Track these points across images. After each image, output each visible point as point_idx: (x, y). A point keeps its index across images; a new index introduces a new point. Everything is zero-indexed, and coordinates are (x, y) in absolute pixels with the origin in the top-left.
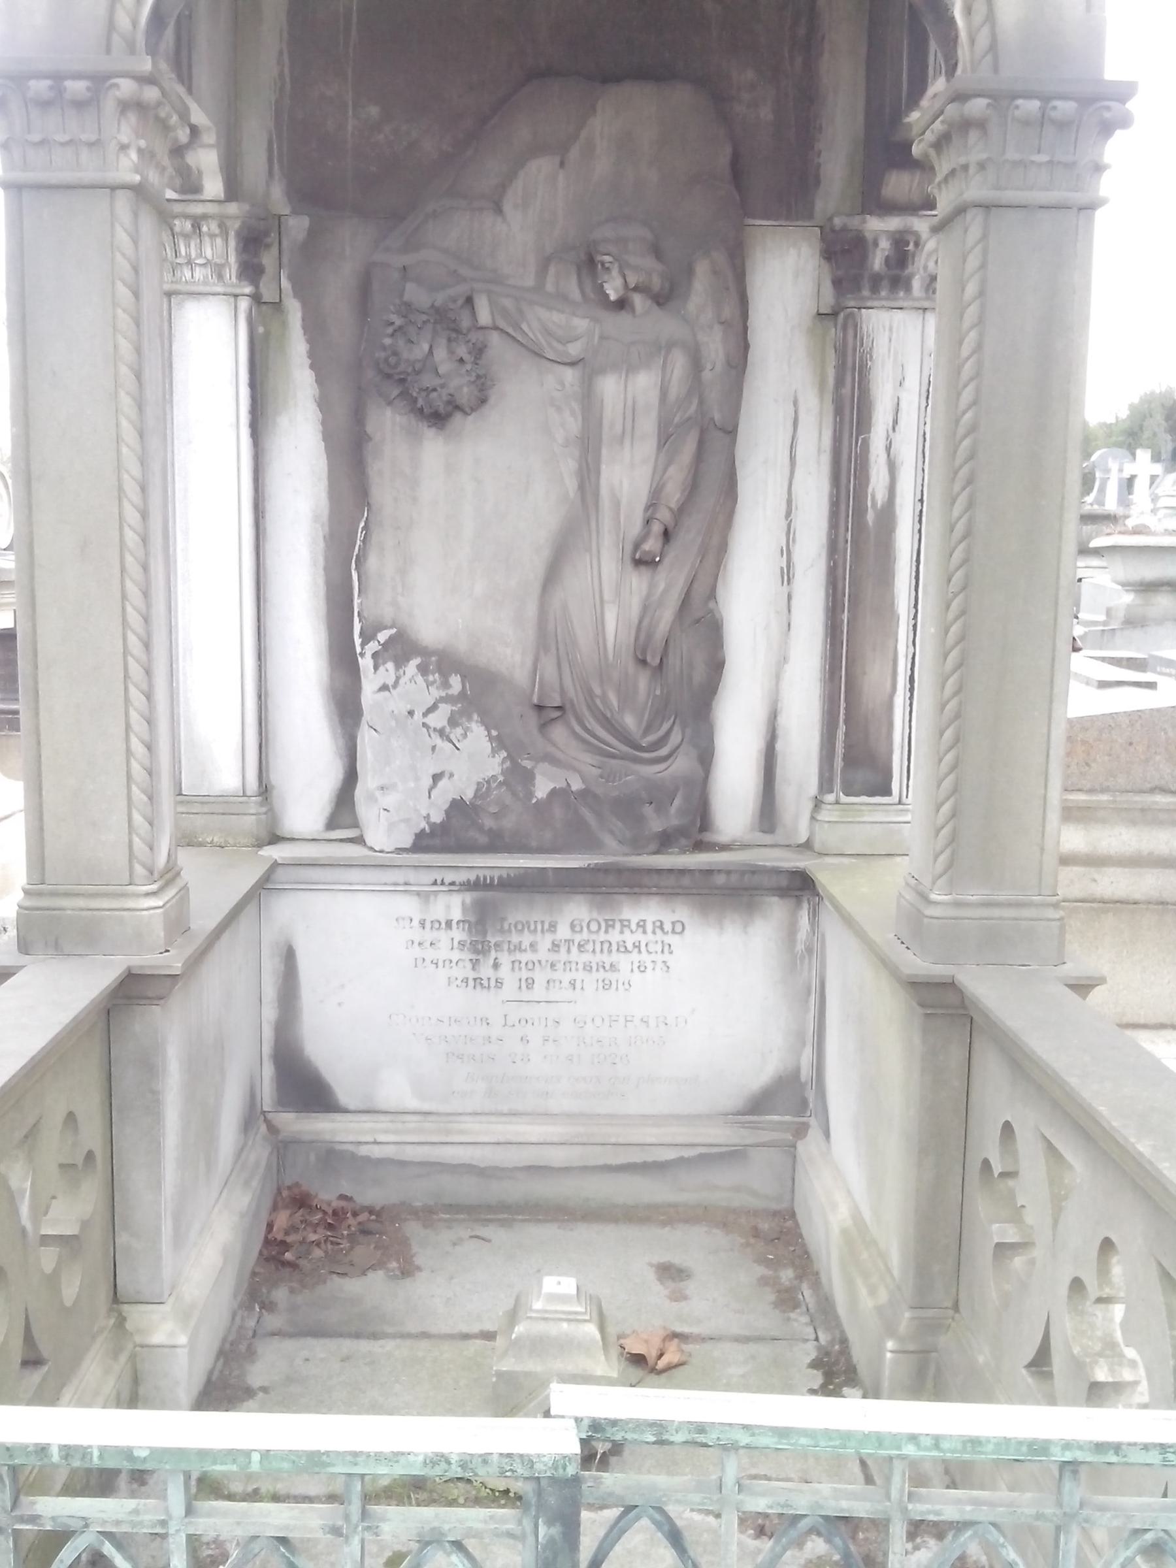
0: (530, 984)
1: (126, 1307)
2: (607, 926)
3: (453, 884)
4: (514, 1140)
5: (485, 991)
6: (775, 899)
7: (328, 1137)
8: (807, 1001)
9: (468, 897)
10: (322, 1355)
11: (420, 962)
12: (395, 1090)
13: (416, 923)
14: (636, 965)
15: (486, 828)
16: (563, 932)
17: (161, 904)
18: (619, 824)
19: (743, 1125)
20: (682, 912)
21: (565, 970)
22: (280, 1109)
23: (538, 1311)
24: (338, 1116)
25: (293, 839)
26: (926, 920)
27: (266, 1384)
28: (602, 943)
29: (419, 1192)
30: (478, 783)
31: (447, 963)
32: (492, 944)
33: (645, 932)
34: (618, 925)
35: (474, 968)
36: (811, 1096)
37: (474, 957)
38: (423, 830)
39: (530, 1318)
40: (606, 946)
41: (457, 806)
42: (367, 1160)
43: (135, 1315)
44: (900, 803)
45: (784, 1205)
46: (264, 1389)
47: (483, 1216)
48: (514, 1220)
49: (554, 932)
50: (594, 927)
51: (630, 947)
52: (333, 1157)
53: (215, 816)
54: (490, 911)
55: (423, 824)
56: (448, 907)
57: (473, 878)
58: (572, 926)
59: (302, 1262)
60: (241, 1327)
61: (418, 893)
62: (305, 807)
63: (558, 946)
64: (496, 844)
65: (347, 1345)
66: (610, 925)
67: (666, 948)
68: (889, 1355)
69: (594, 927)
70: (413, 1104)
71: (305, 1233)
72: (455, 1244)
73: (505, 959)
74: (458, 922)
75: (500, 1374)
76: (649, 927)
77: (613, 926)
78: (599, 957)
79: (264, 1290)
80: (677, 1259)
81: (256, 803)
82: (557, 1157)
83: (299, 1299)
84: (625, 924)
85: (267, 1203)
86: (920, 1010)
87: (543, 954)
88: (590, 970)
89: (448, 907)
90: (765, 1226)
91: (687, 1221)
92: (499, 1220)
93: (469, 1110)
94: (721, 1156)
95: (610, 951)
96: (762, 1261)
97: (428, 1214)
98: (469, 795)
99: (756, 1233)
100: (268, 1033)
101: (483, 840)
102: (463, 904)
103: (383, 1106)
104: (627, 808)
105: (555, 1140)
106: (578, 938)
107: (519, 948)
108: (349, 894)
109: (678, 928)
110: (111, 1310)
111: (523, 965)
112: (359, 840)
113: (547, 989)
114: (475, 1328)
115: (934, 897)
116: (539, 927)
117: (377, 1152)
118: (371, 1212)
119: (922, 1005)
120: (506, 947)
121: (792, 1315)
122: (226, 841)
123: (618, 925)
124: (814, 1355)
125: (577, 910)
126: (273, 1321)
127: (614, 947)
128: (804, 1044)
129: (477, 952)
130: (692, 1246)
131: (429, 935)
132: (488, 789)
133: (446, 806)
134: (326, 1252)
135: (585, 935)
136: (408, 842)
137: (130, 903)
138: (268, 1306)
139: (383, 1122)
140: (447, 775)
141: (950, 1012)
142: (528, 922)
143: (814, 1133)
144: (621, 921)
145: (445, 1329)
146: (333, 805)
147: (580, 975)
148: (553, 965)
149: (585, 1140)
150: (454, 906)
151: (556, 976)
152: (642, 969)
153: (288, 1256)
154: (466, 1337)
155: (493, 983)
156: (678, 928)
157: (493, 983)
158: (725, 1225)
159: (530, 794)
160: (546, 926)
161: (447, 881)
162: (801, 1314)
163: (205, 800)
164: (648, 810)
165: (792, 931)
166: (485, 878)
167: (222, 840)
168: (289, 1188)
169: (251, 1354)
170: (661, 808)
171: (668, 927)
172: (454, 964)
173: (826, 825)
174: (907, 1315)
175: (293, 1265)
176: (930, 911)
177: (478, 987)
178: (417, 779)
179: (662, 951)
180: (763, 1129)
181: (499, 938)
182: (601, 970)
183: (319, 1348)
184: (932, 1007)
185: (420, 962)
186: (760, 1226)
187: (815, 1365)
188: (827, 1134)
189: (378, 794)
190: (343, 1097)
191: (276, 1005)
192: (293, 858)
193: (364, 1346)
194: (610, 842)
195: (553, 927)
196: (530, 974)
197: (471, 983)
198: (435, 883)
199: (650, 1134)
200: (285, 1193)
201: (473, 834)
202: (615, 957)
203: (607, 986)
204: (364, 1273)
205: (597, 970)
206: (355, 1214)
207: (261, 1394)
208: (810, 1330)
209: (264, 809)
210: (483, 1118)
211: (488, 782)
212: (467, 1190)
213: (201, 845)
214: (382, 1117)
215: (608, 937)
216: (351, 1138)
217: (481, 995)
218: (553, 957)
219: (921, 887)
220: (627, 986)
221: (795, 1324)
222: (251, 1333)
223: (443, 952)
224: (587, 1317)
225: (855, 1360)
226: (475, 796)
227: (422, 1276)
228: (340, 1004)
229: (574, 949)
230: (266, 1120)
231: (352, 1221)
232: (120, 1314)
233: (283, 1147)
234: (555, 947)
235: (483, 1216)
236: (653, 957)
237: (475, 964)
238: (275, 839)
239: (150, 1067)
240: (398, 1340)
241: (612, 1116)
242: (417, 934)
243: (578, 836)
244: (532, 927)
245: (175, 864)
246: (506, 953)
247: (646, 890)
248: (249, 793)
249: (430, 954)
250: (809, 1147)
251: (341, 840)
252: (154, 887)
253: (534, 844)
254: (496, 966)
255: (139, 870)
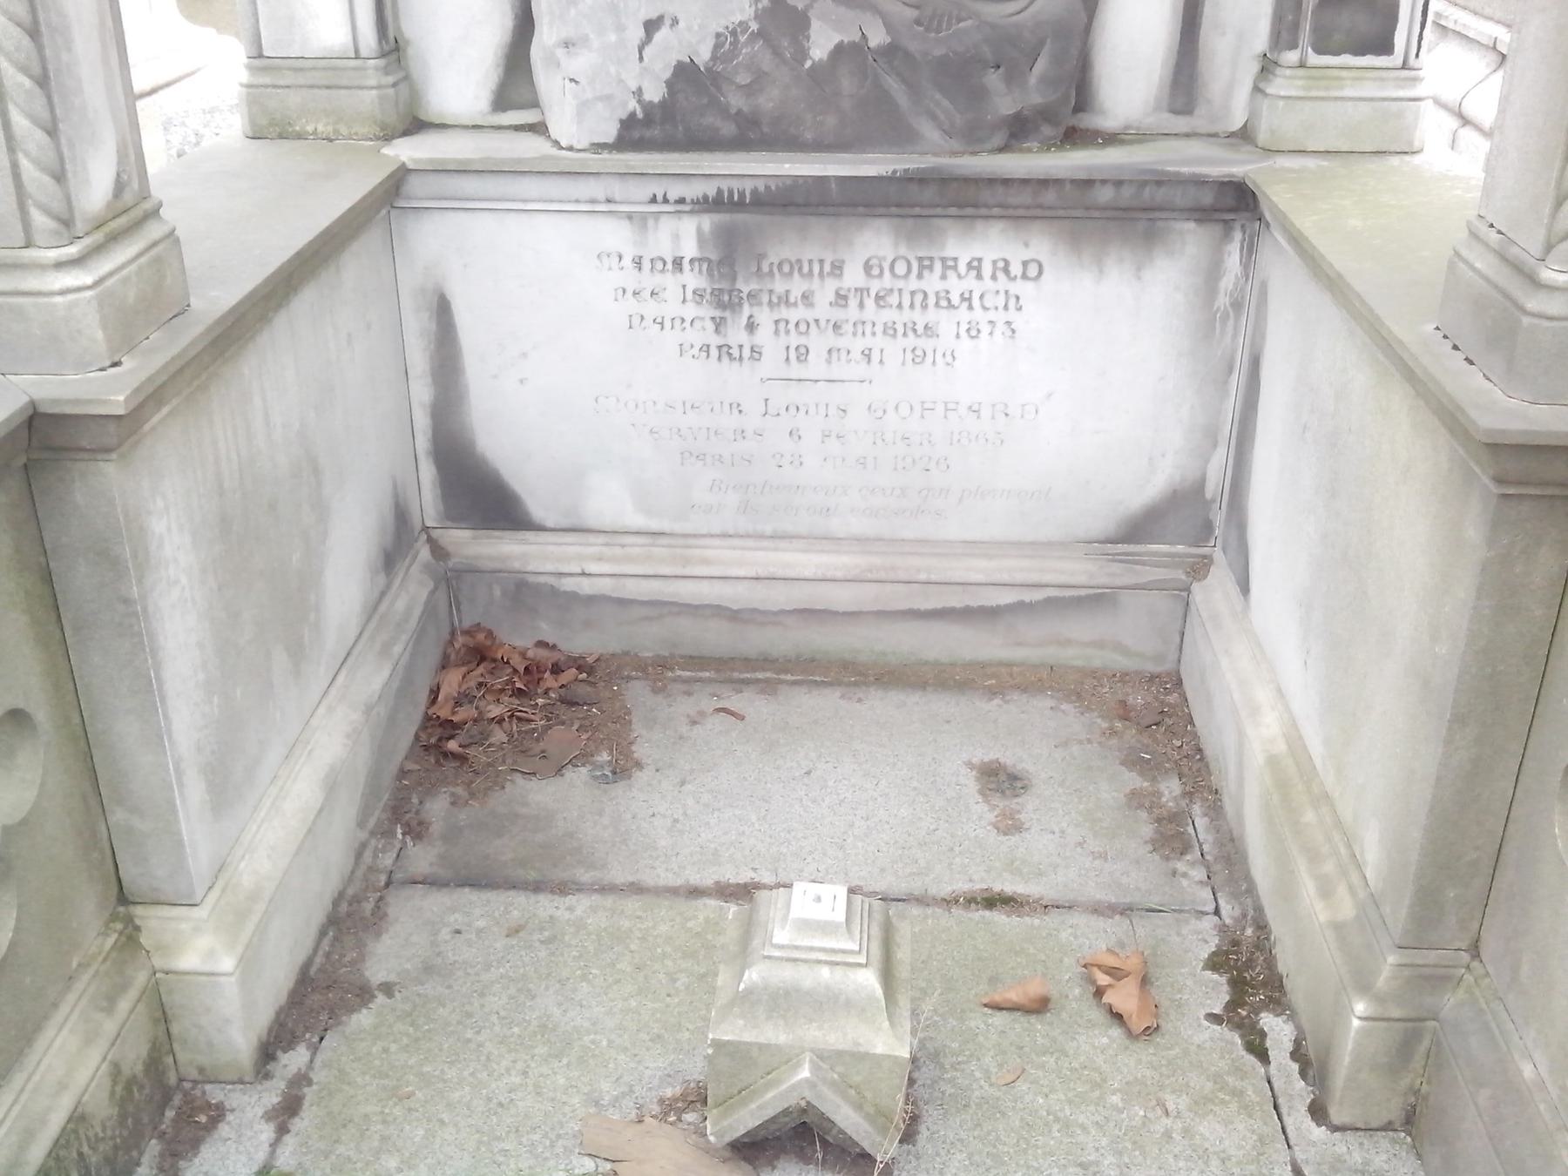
0: (803, 354)
1: (139, 911)
2: (921, 268)
3: (681, 201)
4: (780, 573)
5: (736, 364)
6: (1191, 225)
7: (517, 565)
8: (1226, 382)
9: (707, 222)
10: (481, 923)
11: (636, 321)
12: (610, 501)
13: (627, 261)
14: (964, 327)
15: (733, 111)
16: (853, 276)
17: (88, 279)
18: (946, 103)
19: (1115, 558)
20: (1039, 245)
21: (854, 334)
22: (449, 524)
23: (782, 947)
24: (530, 535)
25: (443, 126)
26: (1526, 320)
27: (392, 978)
28: (913, 293)
29: (648, 639)
30: (718, 35)
31: (677, 322)
32: (744, 295)
33: (979, 277)
34: (938, 266)
35: (717, 331)
36: (1219, 518)
37: (718, 313)
38: (633, 115)
39: (769, 957)
40: (919, 298)
41: (685, 73)
42: (573, 597)
43: (152, 920)
44: (1405, 66)
45: (1168, 666)
46: (388, 989)
47: (736, 675)
48: (781, 682)
49: (841, 275)
50: (901, 268)
51: (955, 300)
52: (525, 592)
53: (316, 91)
54: (741, 237)
55: (633, 105)
56: (676, 237)
57: (712, 193)
58: (867, 268)
59: (471, 751)
60: (371, 869)
61: (630, 216)
62: (459, 77)
63: (845, 298)
64: (751, 134)
65: (520, 904)
66: (925, 265)
67: (1012, 301)
68: (1356, 1023)
69: (901, 268)
70: (638, 521)
71: (482, 704)
72: (694, 723)
73: (765, 317)
74: (692, 261)
75: (717, 1044)
76: (987, 270)
77: (931, 268)
78: (907, 315)
79: (415, 800)
80: (1008, 756)
81: (376, 69)
82: (842, 598)
83: (463, 816)
84: (949, 265)
85: (433, 657)
86: (1495, 490)
87: (823, 307)
88: (894, 336)
89: (676, 237)
90: (1137, 700)
91: (1024, 688)
92: (758, 681)
93: (716, 530)
94: (1078, 602)
95: (924, 307)
96: (1133, 762)
97: (661, 670)
98: (703, 55)
99: (1125, 712)
100: (422, 421)
101: (728, 129)
102: (699, 231)
103: (592, 523)
104: (960, 75)
105: (839, 575)
106: (875, 286)
107: (785, 300)
108: (524, 216)
109: (1033, 271)
110: (114, 917)
111: (791, 326)
112: (539, 128)
113: (829, 362)
114: (707, 878)
115: (1547, 275)
116: (816, 269)
117: (586, 587)
118: (580, 669)
119: (1499, 481)
120: (765, 299)
121: (1181, 866)
122: (336, 131)
123: (938, 266)
124: (1213, 944)
125: (875, 241)
126: (422, 858)
127: (932, 300)
128: (1215, 445)
129: (721, 305)
130: (1036, 734)
131: (649, 280)
132: (735, 43)
133: (668, 74)
134: (510, 735)
135: (887, 280)
136: (610, 133)
137: (32, 282)
138: (417, 831)
139: (594, 545)
140: (668, 22)
141: (1549, 491)
142: (799, 261)
143: (1220, 579)
144: (943, 260)
145: (666, 878)
146: (500, 70)
147: (879, 342)
148: (836, 327)
149: (882, 575)
150: (685, 236)
151: (842, 342)
152: (973, 332)
153: (452, 745)
154: (695, 892)
155: (746, 352)
156: (1033, 271)
157: (746, 352)
158: (1076, 696)
159: (803, 54)
160: (827, 268)
161: (672, 196)
162: (1192, 864)
163: (299, 65)
164: (993, 79)
165: (1213, 273)
166: (731, 192)
167: (330, 128)
168: (467, 633)
169: (377, 921)
170: (1014, 77)
171: (1016, 269)
172: (687, 324)
173: (1281, 103)
174: (1391, 959)
175: (462, 759)
176: (1534, 303)
177: (725, 359)
178: (620, 28)
179: (1006, 307)
180: (1143, 563)
181: (754, 286)
182: (910, 333)
183: (480, 908)
184: (1519, 483)
185: (636, 321)
186: (1130, 700)
187: (1216, 963)
188: (1245, 587)
189: (560, 53)
190: (537, 509)
191: (429, 380)
192: (431, 161)
193: (546, 906)
194: (930, 132)
195: (838, 269)
196: (803, 340)
197: (714, 352)
198: (654, 200)
199: (976, 569)
200: (460, 640)
201: (710, 120)
202: (932, 315)
203: (919, 357)
204: (559, 771)
205: (905, 334)
206: (557, 670)
207: (381, 998)
208: (1206, 894)
209: (391, 79)
210: (736, 542)
211: (734, 33)
212: (716, 638)
213: (300, 136)
214: (592, 538)
215: (923, 285)
216: (549, 567)
217: (729, 369)
218: (838, 314)
219: (1515, 250)
220: (949, 359)
221: (1185, 883)
222: (383, 878)
223: (672, 306)
224: (864, 961)
225: (1281, 968)
226: (714, 58)
227: (641, 777)
228: (521, 381)
229: (870, 303)
230: (430, 540)
231: (549, 680)
232: (129, 920)
233: (452, 579)
234: (841, 299)
235: (736, 675)
236: (992, 315)
237: (719, 324)
238: (416, 125)
239: (118, 557)
240: (595, 897)
241: (923, 542)
242: (630, 279)
243: (879, 124)
244: (806, 269)
245: (145, 195)
246: (766, 308)
247: (983, 211)
248: (364, 53)
249: (651, 309)
250: (1214, 592)
251: (518, 128)
252: (73, 250)
253: (809, 136)
254: (751, 327)
255: (39, 219)
